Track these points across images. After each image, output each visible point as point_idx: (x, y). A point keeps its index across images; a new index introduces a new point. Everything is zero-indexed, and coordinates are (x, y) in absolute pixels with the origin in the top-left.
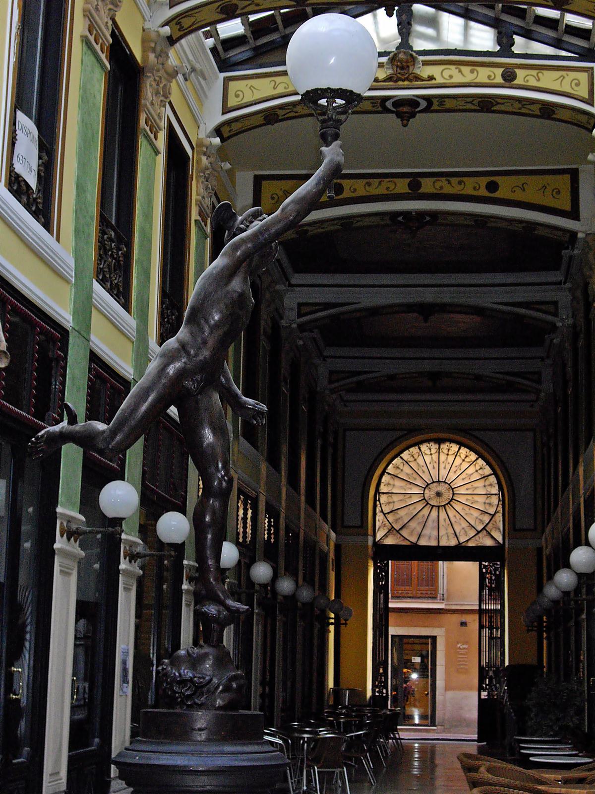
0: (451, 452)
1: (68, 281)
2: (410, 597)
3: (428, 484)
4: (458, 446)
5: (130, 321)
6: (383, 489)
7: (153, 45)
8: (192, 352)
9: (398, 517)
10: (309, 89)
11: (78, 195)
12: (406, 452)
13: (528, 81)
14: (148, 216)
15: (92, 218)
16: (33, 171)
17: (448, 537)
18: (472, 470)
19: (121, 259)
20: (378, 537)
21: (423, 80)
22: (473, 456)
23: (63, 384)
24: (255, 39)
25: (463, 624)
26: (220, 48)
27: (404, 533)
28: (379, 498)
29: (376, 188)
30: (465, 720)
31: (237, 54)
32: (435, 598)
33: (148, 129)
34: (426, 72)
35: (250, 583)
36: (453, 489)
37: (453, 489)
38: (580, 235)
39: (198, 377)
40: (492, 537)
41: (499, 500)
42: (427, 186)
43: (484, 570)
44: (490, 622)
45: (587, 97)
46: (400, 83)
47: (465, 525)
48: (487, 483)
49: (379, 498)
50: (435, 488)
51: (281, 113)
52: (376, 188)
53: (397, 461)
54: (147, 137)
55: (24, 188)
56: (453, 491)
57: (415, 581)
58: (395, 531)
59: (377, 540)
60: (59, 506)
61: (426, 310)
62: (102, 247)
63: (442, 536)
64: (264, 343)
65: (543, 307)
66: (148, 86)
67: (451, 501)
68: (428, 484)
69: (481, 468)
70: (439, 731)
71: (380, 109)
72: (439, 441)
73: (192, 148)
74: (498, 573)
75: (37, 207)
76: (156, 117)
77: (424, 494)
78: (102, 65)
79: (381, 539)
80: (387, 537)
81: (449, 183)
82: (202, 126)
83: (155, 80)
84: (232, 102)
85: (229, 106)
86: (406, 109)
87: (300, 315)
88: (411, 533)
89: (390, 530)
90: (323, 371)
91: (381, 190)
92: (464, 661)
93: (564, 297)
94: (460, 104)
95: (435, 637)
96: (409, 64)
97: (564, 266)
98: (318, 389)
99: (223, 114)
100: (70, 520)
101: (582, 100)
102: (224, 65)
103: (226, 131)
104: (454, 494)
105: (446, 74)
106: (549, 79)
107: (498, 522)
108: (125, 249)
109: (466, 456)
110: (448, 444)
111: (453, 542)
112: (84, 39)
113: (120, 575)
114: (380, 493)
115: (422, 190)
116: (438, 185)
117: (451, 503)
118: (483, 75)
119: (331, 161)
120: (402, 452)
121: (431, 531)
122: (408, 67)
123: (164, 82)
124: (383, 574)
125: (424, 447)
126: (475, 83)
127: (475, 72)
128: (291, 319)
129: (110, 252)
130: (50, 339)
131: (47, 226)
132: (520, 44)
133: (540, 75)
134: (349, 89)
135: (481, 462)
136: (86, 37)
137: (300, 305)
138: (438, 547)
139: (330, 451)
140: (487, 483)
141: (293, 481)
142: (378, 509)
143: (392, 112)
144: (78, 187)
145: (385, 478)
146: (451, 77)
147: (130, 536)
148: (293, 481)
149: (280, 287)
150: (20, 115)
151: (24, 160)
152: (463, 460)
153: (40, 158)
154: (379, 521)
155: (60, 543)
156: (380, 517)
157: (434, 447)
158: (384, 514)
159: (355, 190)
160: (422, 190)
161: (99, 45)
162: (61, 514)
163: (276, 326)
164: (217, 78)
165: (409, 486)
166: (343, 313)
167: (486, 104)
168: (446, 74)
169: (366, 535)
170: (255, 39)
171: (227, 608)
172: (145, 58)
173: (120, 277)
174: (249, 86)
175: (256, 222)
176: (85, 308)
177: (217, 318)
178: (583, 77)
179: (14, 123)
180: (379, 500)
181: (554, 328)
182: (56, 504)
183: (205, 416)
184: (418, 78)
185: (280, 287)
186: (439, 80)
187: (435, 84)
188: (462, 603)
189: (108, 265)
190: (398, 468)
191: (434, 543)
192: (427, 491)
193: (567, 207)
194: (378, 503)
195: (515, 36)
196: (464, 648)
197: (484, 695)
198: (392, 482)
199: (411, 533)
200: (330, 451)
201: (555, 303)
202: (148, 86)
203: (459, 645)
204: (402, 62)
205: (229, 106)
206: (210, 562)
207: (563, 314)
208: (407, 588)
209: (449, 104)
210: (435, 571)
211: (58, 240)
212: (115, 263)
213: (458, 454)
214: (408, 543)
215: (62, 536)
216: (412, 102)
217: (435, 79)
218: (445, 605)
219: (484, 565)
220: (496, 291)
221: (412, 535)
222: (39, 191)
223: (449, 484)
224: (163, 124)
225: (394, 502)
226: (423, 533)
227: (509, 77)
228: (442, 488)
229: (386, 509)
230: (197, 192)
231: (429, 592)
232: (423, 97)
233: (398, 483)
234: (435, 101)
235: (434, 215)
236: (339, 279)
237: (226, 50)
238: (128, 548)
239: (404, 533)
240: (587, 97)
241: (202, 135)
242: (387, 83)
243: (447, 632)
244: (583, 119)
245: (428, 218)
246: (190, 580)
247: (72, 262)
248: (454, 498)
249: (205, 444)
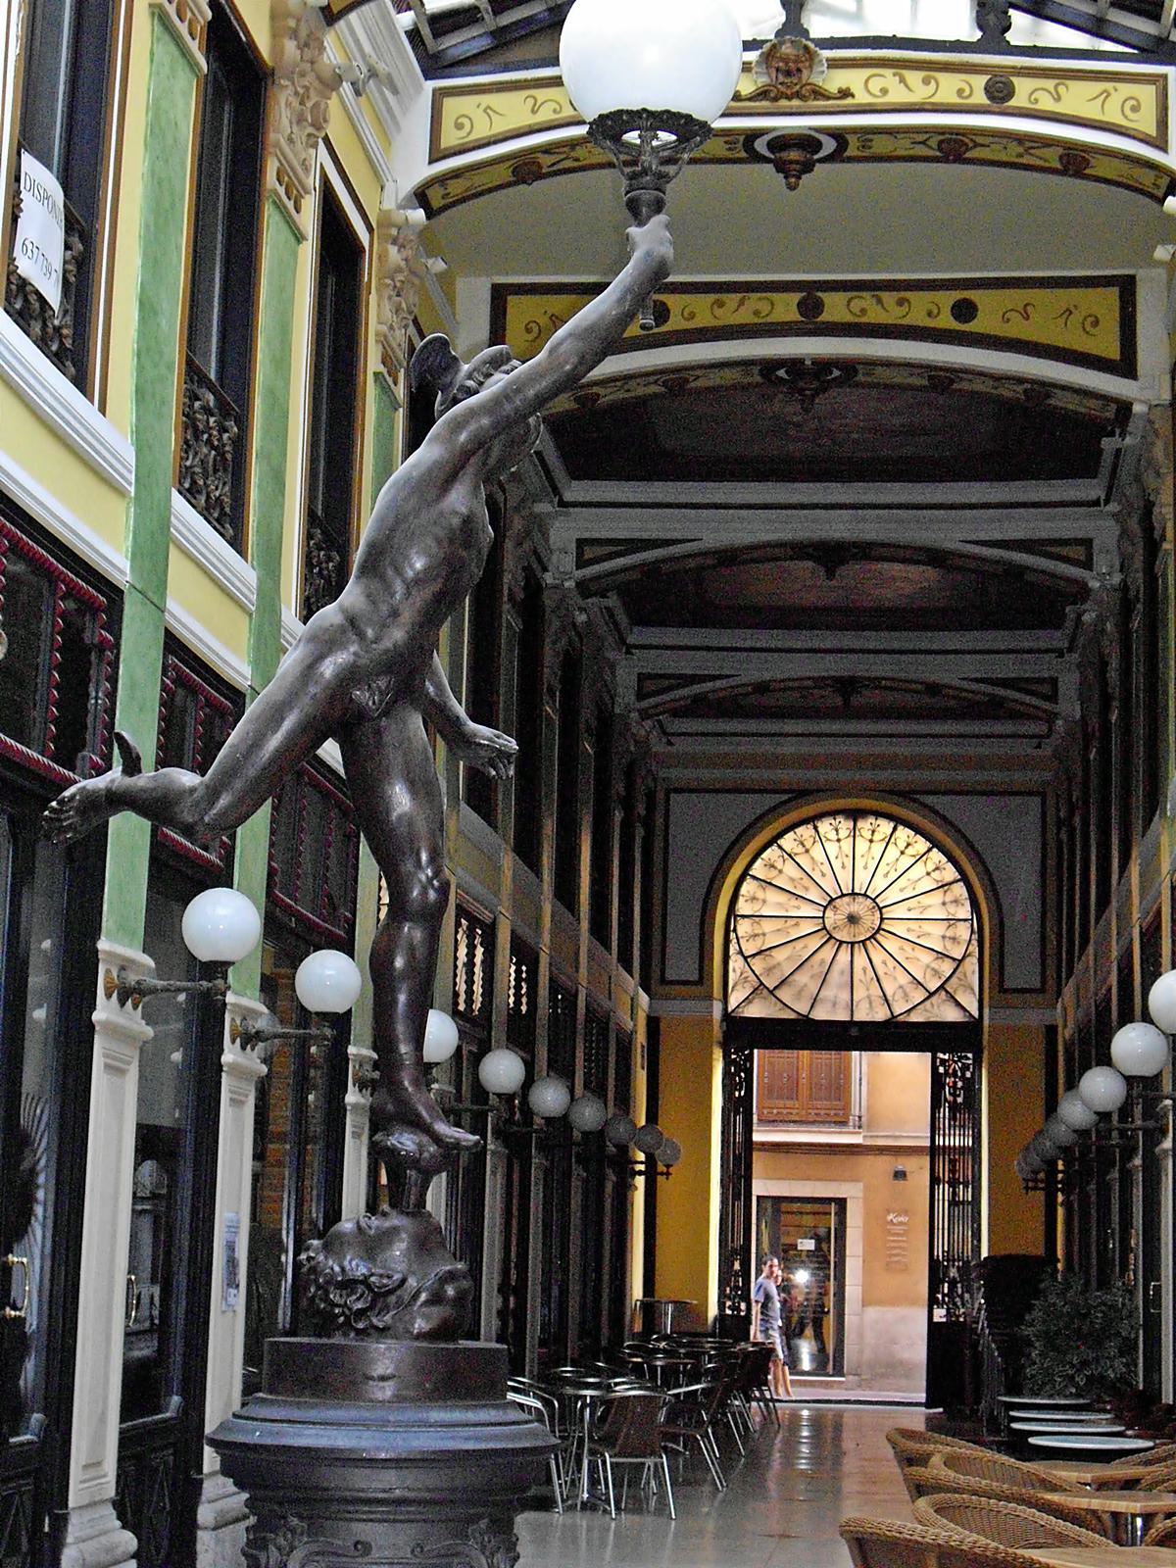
0: (877, 837)
1: (121, 492)
2: (794, 1122)
3: (832, 900)
4: (892, 825)
5: (244, 573)
6: (743, 907)
7: (292, 23)
8: (370, 633)
10: (605, 111)
11: (143, 320)
12: (790, 836)
13: (1036, 101)
14: (282, 363)
15: (170, 368)
16: (53, 272)
17: (870, 1003)
18: (919, 870)
19: (227, 448)
20: (733, 1003)
21: (829, 98)
22: (922, 845)
23: (112, 695)
24: (496, 12)
25: (900, 1175)
26: (426, 31)
27: (784, 994)
28: (735, 926)
29: (735, 311)
30: (901, 1363)
31: (458, 43)
32: (844, 1123)
33: (281, 191)
34: (835, 81)
35: (480, 1092)
36: (880, 909)
38: (1137, 408)
39: (382, 683)
40: (958, 1004)
41: (972, 932)
42: (836, 308)
43: (941, 1070)
44: (953, 1171)
45: (1154, 135)
46: (784, 103)
47: (904, 979)
48: (949, 898)
49: (735, 926)
50: (846, 906)
51: (546, 160)
52: (735, 311)
53: (771, 853)
54: (279, 206)
55: (37, 305)
56: (881, 914)
57: (804, 1091)
58: (765, 991)
59: (730, 1010)
60: (103, 938)
61: (831, 555)
62: (190, 425)
64: (509, 619)
65: (1064, 551)
66: (283, 105)
67: (877, 932)
68: (832, 900)
69: (937, 869)
70: (850, 1385)
71: (743, 154)
72: (855, 815)
73: (370, 229)
74: (968, 1075)
75: (62, 343)
76: (299, 169)
77: (823, 918)
78: (192, 64)
79: (738, 1007)
80: (750, 1002)
81: (879, 301)
82: (389, 185)
83: (296, 93)
84: (450, 138)
85: (442, 146)
86: (794, 156)
87: (581, 563)
88: (798, 995)
89: (756, 989)
90: (625, 676)
91: (744, 317)
92: (900, 1248)
93: (1104, 531)
94: (903, 147)
95: (844, 1200)
96: (800, 65)
97: (1105, 470)
98: (617, 711)
99: (431, 162)
100: (125, 965)
101: (1145, 140)
102: (434, 65)
103: (436, 198)
104: (882, 919)
105: (875, 85)
106: (1078, 98)
107: (969, 974)
108: (236, 429)
109: (908, 845)
110: (871, 819)
111: (881, 1015)
112: (156, 11)
113: (223, 1074)
114: (736, 916)
115: (826, 317)
116: (856, 305)
117: (878, 936)
118: (948, 88)
119: (648, 254)
120: (780, 835)
121: (835, 991)
122: (799, 70)
123: (314, 98)
124: (743, 1075)
125: (825, 826)
126: (933, 104)
127: (933, 82)
128: (562, 570)
129: (205, 436)
130: (88, 607)
131: (81, 382)
132: (1022, 27)
133: (1061, 89)
134: (684, 111)
135: (936, 856)
136: (160, 7)
137: (581, 543)
138: (852, 1023)
139: (640, 832)
140: (949, 898)
141: (566, 893)
142: (733, 948)
143: (767, 160)
144: (141, 303)
145: (748, 887)
146: (884, 91)
147: (243, 998)
148: (566, 893)
149: (543, 507)
150: (28, 162)
151: (35, 250)
153: (67, 247)
154: (734, 970)
155: (104, 1011)
156: (736, 963)
157: (845, 825)
158: (746, 958)
159: (692, 316)
160: (826, 317)
161: (187, 23)
162: (105, 952)
163: (533, 587)
164: (419, 89)
165: (794, 902)
166: (672, 559)
167: (954, 147)
168: (875, 85)
169: (710, 997)
170: (496, 12)
171: (437, 1139)
172: (277, 49)
173: (224, 484)
174: (483, 107)
175: (497, 376)
176: (155, 543)
177: (419, 565)
178: (1147, 94)
179: (15, 177)
180: (735, 930)
181: (1082, 592)
182: (95, 932)
183: (395, 759)
184: (818, 93)
185: (543, 507)
186: (861, 98)
187: (853, 105)
188: (897, 1134)
189: (202, 461)
190: (773, 866)
191: (842, 1016)
192: (829, 913)
193: (1113, 352)
194: (732, 935)
195: (1012, 12)
196: (901, 1223)
197: (940, 1315)
198: (760, 894)
199: (798, 995)
200: (640, 832)
201: (1087, 543)
202: (283, 105)
203: (890, 1218)
205: (442, 146)
206: (404, 1049)
207: (1102, 563)
208: (789, 1103)
209: (881, 145)
210: (845, 1071)
211: (103, 410)
212: (215, 460)
213: (893, 840)
214: (793, 1016)
215: (109, 996)
216: (807, 142)
217: (853, 96)
218: (865, 1137)
219: (942, 1060)
220: (973, 518)
221: (799, 999)
222: (66, 312)
223: (874, 900)
224: (313, 181)
225: (764, 934)
226: (821, 996)
227: (999, 93)
228: (860, 907)
229: (749, 948)
230: (378, 317)
231: (832, 1112)
233: (772, 896)
234: (852, 140)
236: (660, 491)
237: (437, 34)
238: (238, 1022)
239: (784, 994)
240: (1154, 135)
241: (389, 204)
242: (757, 104)
243: (867, 1189)
244: (1147, 178)
245: (836, 373)
246: (362, 1084)
247: (130, 455)
248: (883, 926)
249: (394, 815)
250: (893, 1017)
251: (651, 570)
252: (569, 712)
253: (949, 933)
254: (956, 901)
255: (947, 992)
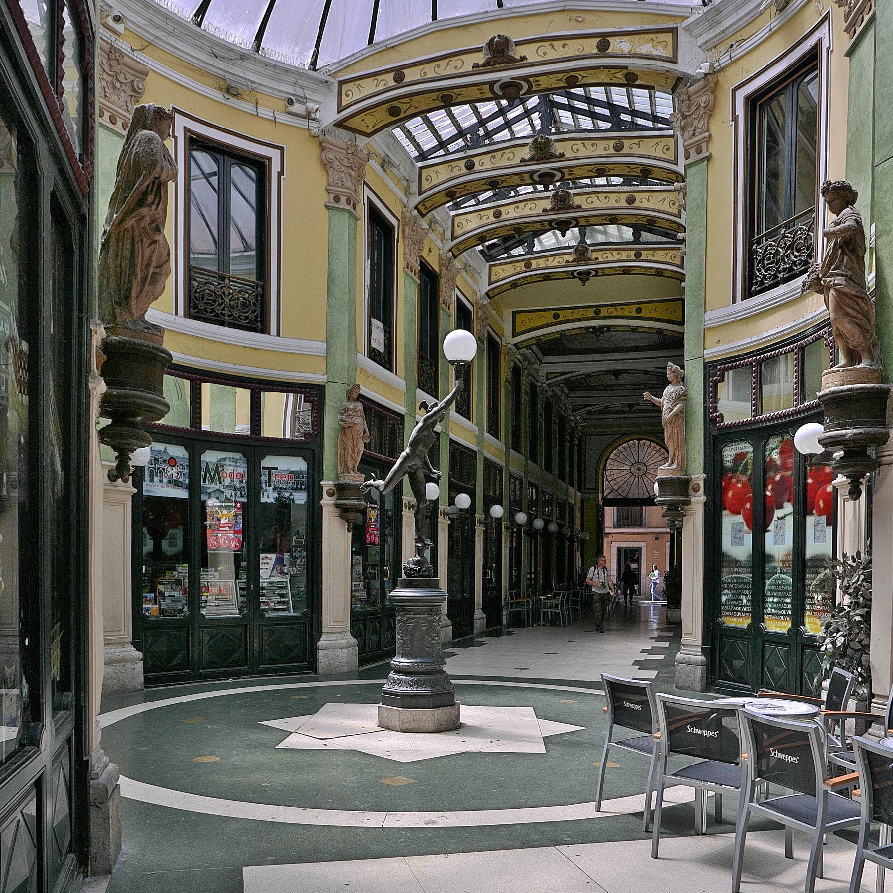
26: (486, 251)
34: (595, 255)
61: (616, 373)
64: (525, 398)
78: (415, 282)
84: (493, 278)
86: (584, 277)
91: (580, 316)
94: (613, 272)
101: (677, 266)
128: (543, 382)
147: (443, 507)
149: (536, 366)
163: (533, 387)
179: (370, 324)
184: (590, 260)
185: (536, 366)
186: (601, 260)
204: (581, 252)
209: (607, 272)
216: (587, 273)
224: (454, 299)
232: (592, 270)
235: (609, 328)
251: (567, 381)
252: (548, 419)
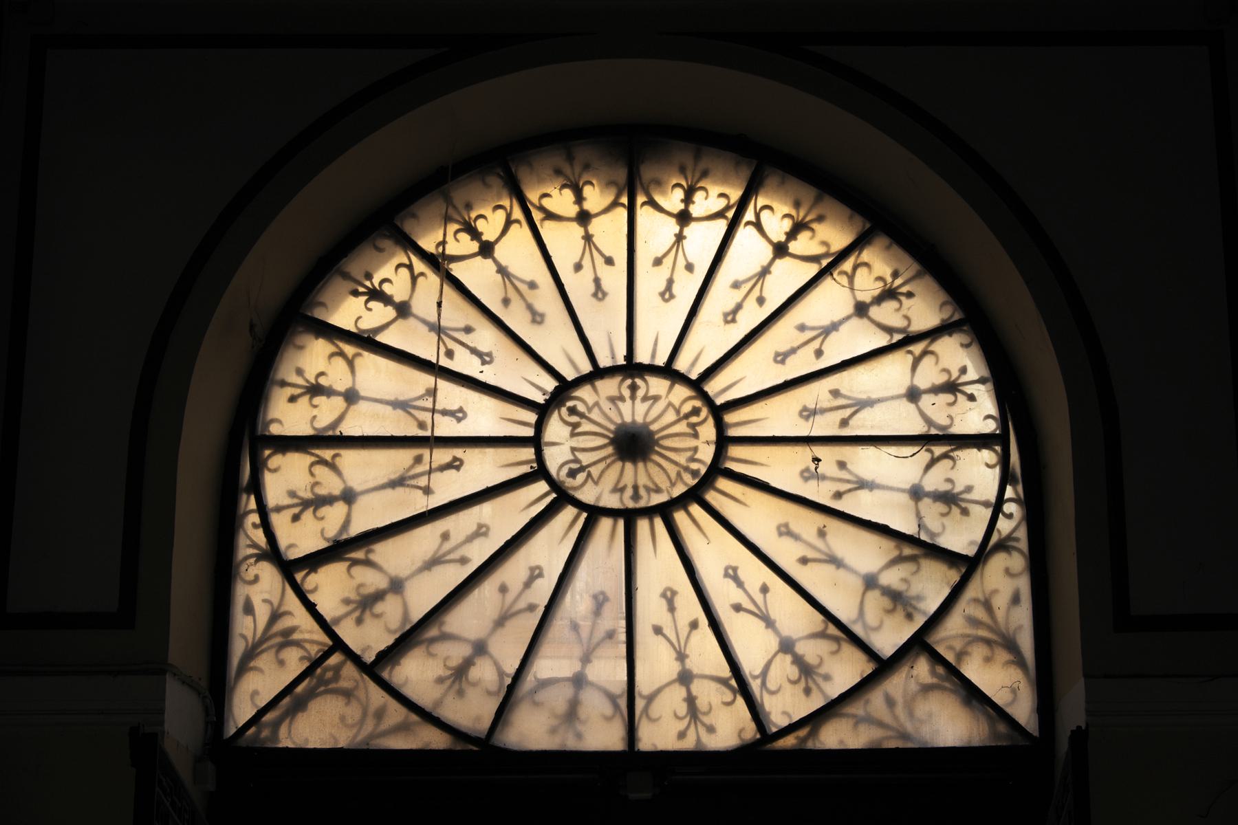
9: (372, 580)
20: (242, 710)
37: (718, 412)
40: (972, 695)
48: (928, 375)
50: (607, 405)
56: (720, 426)
58: (350, 670)
59: (231, 730)
63: (651, 698)
67: (649, 512)
138: (632, 760)
152: (780, 250)
156: (260, 587)
180: (256, 487)
191: (603, 736)
192: (556, 429)
214: (435, 739)
229: (300, 538)
239: (417, 673)
250: (765, 734)
253: (935, 481)
254: (951, 387)
255: (936, 658)
